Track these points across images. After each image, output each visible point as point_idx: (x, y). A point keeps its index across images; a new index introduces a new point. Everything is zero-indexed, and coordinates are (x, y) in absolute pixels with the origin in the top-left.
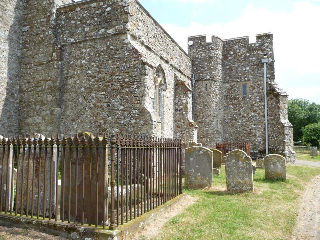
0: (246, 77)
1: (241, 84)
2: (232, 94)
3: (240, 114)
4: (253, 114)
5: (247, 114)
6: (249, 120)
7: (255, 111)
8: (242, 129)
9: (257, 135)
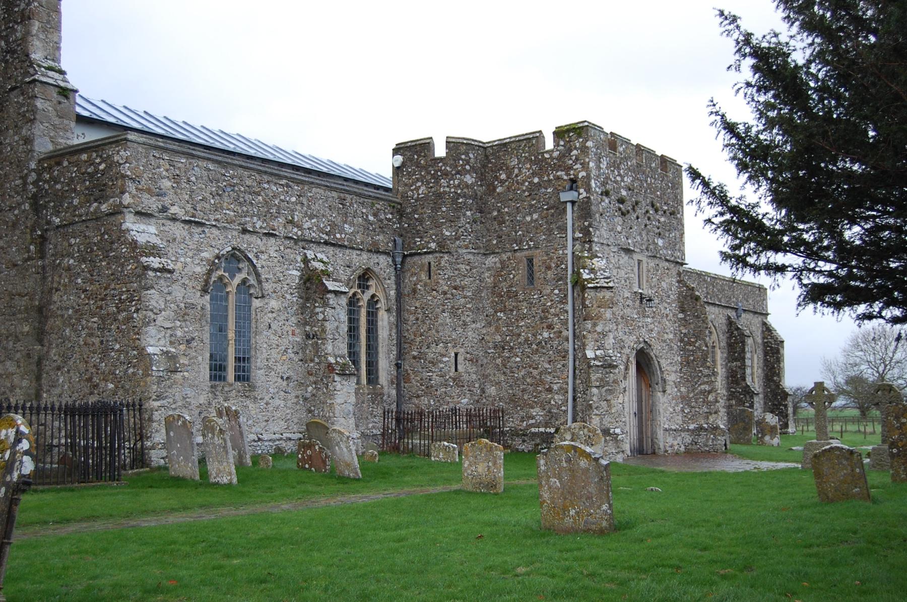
0: (531, 240)
4: (546, 335)
7: (550, 327)
9: (555, 387)
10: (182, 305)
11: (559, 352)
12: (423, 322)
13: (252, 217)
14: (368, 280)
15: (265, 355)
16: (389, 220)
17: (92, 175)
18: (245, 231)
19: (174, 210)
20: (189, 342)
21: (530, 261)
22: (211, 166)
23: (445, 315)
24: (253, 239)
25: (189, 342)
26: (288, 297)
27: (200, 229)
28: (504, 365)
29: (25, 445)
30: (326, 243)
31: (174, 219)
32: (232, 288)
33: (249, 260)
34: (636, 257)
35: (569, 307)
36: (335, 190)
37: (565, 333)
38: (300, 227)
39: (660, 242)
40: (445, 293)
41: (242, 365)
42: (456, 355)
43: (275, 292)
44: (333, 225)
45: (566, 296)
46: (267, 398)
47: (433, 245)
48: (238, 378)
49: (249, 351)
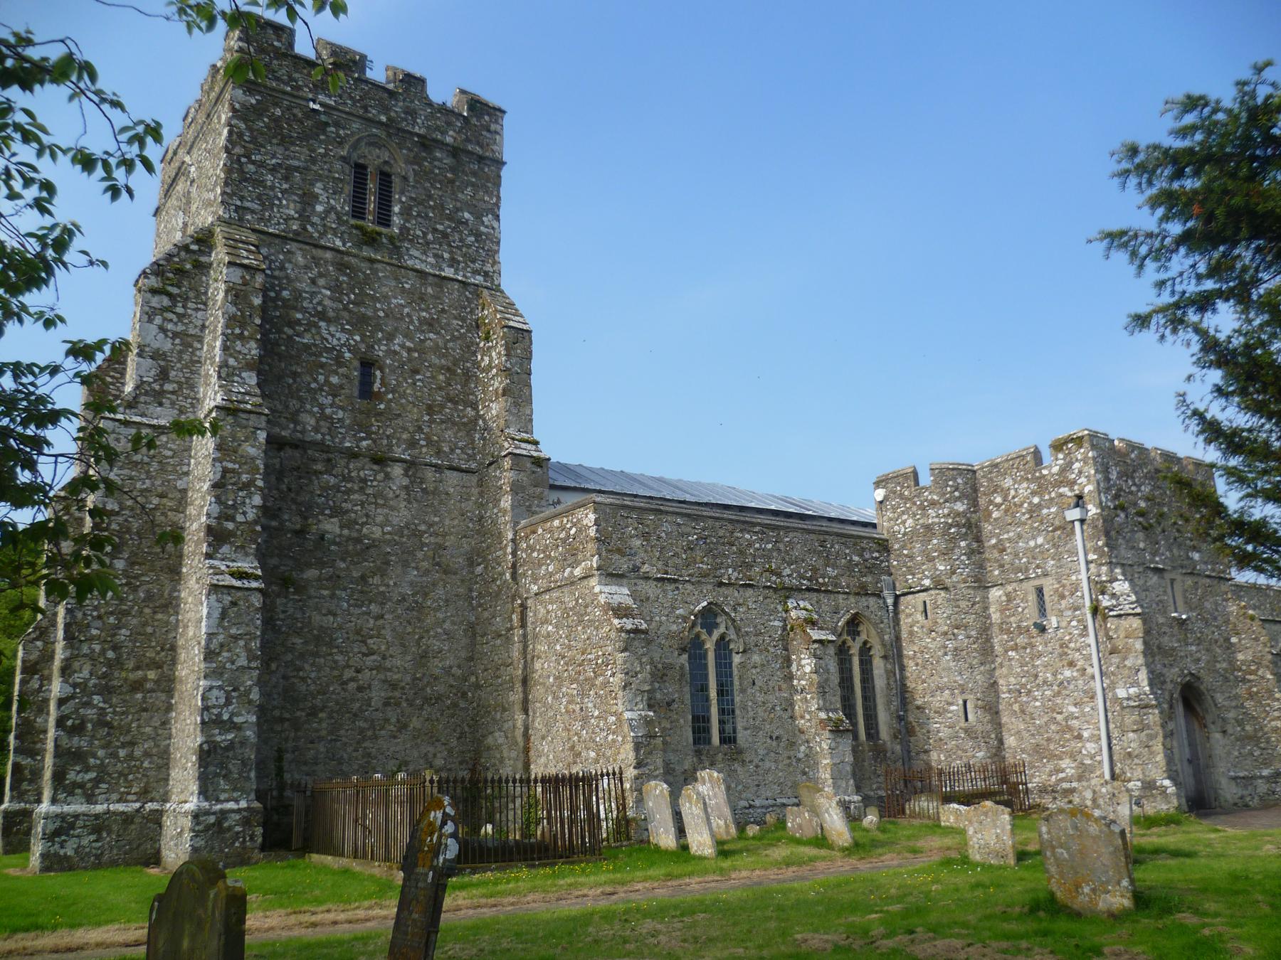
0: (1038, 567)
1: (1029, 586)
2: (1012, 619)
3: (1036, 676)
4: (1068, 673)
5: (1054, 675)
6: (1059, 692)
7: (1071, 664)
8: (1046, 719)
9: (1086, 734)
10: (660, 666)
11: (1085, 692)
12: (924, 667)
13: (727, 568)
14: (858, 625)
16: (876, 559)
17: (564, 541)
18: (721, 584)
19: (646, 568)
20: (669, 704)
21: (1040, 591)
23: (948, 658)
25: (669, 704)
26: (772, 650)
27: (673, 586)
28: (1023, 712)
29: (450, 828)
30: (808, 589)
31: (646, 578)
32: (710, 646)
33: (727, 614)
34: (1168, 576)
35: (1091, 640)
36: (813, 532)
37: (1089, 670)
38: (779, 575)
39: (1196, 556)
40: (946, 634)
42: (965, 702)
44: (815, 570)
45: (1086, 627)
46: (756, 761)
47: (927, 582)
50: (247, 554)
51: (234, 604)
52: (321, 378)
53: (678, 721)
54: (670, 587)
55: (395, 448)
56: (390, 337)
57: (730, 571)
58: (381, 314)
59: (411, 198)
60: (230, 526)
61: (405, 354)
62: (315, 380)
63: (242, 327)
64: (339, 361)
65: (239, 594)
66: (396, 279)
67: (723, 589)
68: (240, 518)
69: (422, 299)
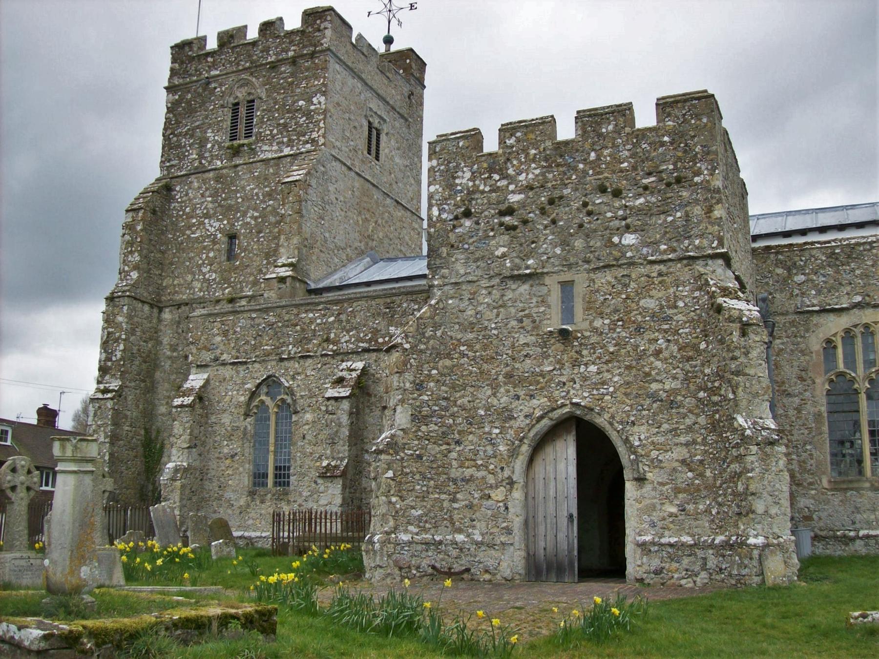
13: (288, 346)
15: (299, 462)
18: (282, 360)
20: (232, 457)
22: (254, 315)
24: (291, 364)
25: (232, 457)
27: (245, 367)
30: (366, 350)
31: (224, 364)
38: (335, 343)
41: (282, 472)
43: (310, 406)
48: (276, 484)
49: (289, 461)
50: (117, 379)
51: (100, 408)
52: (204, 256)
53: (238, 469)
54: (241, 368)
55: (245, 289)
56: (244, 215)
57: (290, 347)
58: (240, 200)
59: (264, 110)
60: (109, 364)
61: (253, 222)
62: (201, 258)
63: (132, 247)
64: (214, 242)
65: (103, 402)
66: (250, 172)
67: (286, 363)
68: (114, 359)
69: (266, 179)
